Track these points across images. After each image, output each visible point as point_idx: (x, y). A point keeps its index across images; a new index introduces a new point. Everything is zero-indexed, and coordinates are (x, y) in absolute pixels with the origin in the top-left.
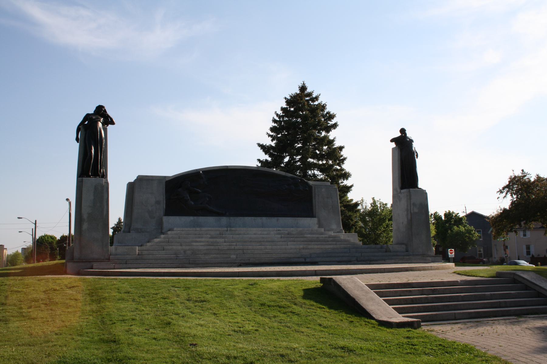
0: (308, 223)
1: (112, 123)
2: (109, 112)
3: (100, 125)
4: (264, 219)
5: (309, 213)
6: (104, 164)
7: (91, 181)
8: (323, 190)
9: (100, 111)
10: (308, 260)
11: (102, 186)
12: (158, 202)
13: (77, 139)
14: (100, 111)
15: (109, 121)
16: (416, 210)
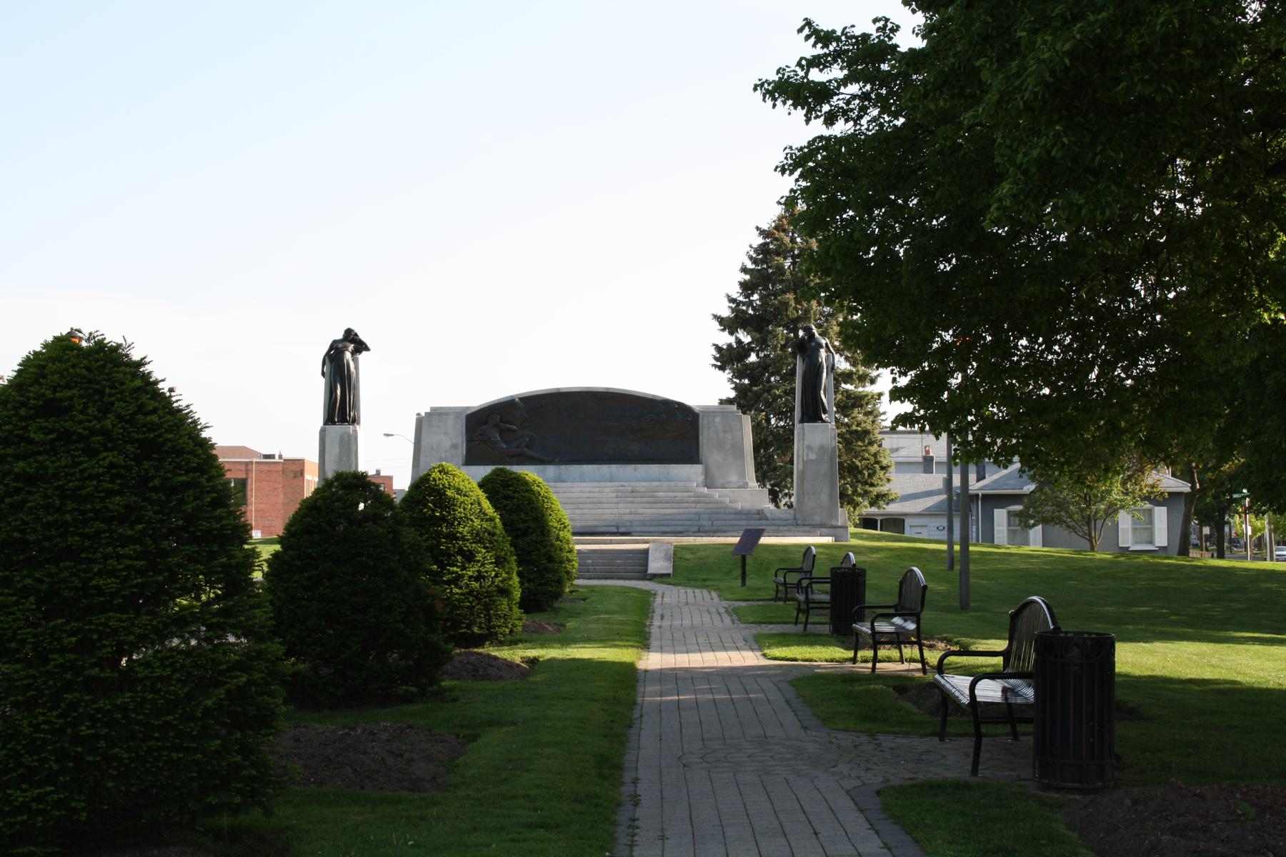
0: (690, 473)
1: (367, 349)
2: (362, 337)
3: (348, 355)
4: (614, 467)
5: (691, 456)
6: (355, 406)
7: (337, 429)
8: (717, 419)
9: (350, 336)
10: (622, 530)
11: (349, 436)
12: (454, 446)
13: (323, 374)
14: (350, 336)
15: (361, 347)
16: (812, 456)
